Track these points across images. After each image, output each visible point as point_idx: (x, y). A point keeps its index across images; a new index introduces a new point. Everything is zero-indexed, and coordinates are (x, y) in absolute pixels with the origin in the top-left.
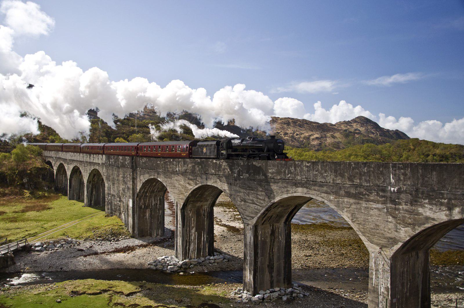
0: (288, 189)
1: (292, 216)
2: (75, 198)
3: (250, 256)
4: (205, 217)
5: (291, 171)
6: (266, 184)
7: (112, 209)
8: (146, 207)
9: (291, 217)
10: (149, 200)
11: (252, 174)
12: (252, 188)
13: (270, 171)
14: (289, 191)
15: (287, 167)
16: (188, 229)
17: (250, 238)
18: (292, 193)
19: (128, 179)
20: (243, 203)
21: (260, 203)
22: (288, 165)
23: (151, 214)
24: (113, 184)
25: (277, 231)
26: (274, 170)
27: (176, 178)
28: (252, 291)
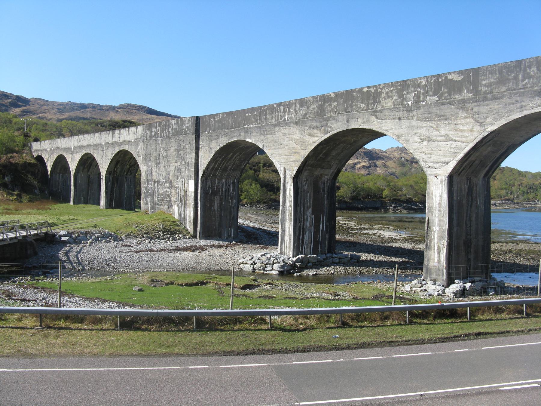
0: (523, 104)
1: (493, 170)
2: (82, 200)
3: (440, 226)
4: (324, 194)
5: (529, 73)
6: (475, 104)
7: (154, 203)
8: (214, 193)
9: (492, 171)
10: (218, 183)
11: (446, 95)
13: (484, 82)
14: (525, 106)
15: (520, 69)
16: (302, 210)
17: (441, 196)
18: (532, 108)
19: (188, 150)
20: (425, 143)
21: (462, 137)
22: (522, 67)
23: (221, 204)
24: (158, 164)
25: (475, 189)
26: (492, 80)
27: (283, 131)
28: (443, 280)
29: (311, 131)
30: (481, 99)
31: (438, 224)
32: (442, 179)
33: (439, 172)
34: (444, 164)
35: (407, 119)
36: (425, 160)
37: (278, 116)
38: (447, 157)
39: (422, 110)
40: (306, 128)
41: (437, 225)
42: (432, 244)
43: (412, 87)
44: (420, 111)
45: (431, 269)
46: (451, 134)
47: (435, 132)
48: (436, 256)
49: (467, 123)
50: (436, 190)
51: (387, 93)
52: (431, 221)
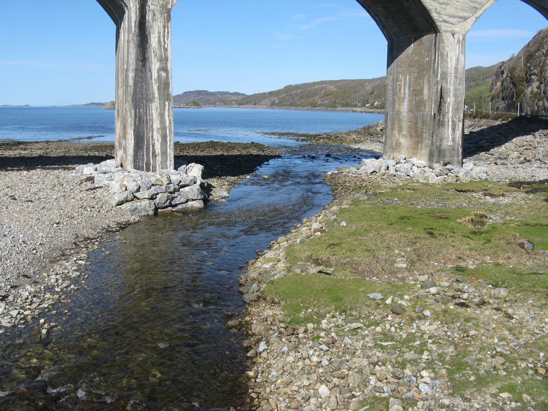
3: (455, 96)
31: (453, 94)
32: (459, 38)
33: (456, 29)
34: (462, 20)
36: (438, 11)
38: (466, 11)
42: (446, 120)
45: (444, 150)
48: (450, 134)
50: (452, 51)
52: (445, 91)
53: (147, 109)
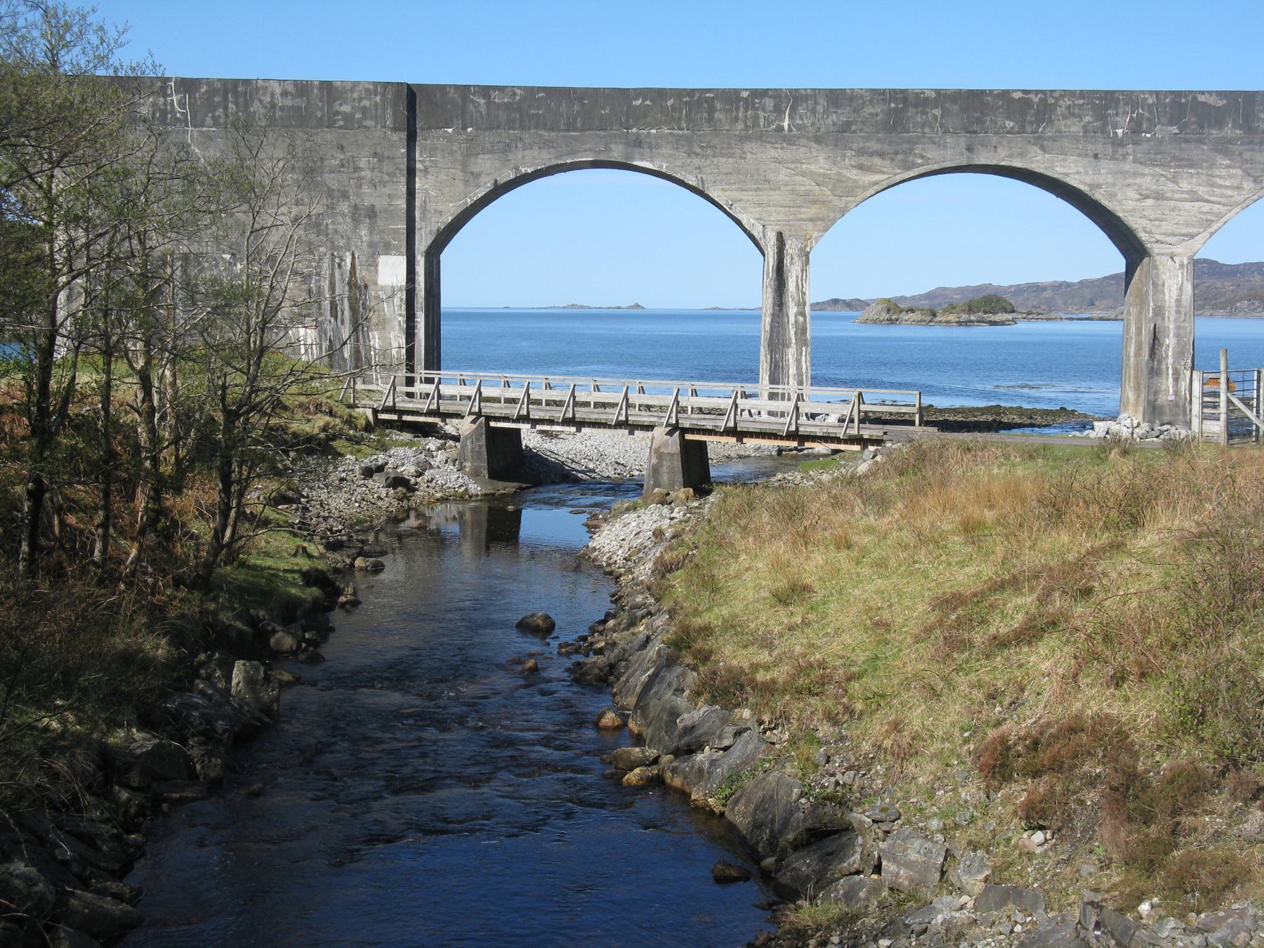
6: (1246, 147)
11: (1194, 127)
12: (1190, 160)
17: (1181, 289)
20: (1149, 202)
21: (1222, 196)
27: (773, 153)
29: (863, 160)
30: (1256, 141)
35: (1113, 158)
37: (756, 118)
38: (1193, 226)
39: (1145, 146)
40: (849, 153)
41: (1172, 335)
42: (1164, 367)
43: (1126, 104)
44: (1141, 147)
45: (1162, 406)
46: (1202, 190)
47: (1171, 185)
49: (1231, 176)
51: (1069, 107)
53: (783, 354)
